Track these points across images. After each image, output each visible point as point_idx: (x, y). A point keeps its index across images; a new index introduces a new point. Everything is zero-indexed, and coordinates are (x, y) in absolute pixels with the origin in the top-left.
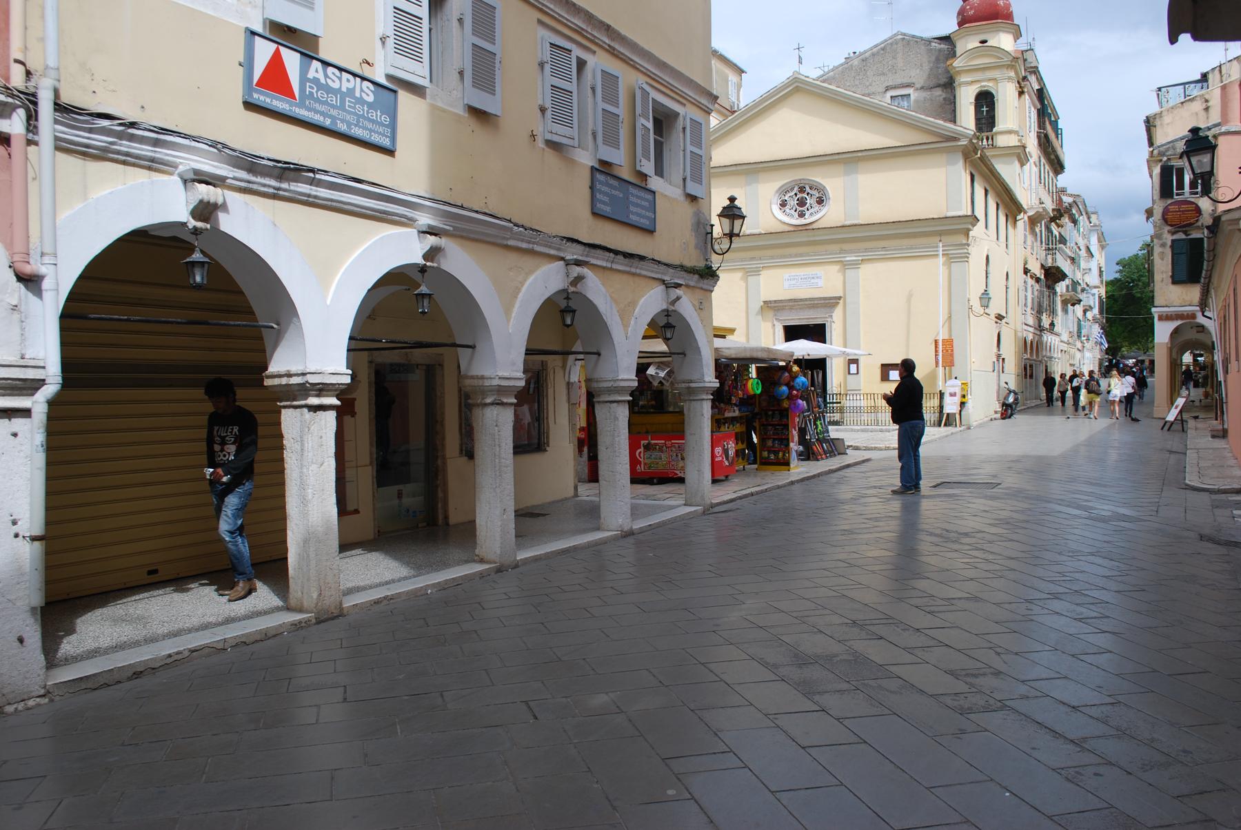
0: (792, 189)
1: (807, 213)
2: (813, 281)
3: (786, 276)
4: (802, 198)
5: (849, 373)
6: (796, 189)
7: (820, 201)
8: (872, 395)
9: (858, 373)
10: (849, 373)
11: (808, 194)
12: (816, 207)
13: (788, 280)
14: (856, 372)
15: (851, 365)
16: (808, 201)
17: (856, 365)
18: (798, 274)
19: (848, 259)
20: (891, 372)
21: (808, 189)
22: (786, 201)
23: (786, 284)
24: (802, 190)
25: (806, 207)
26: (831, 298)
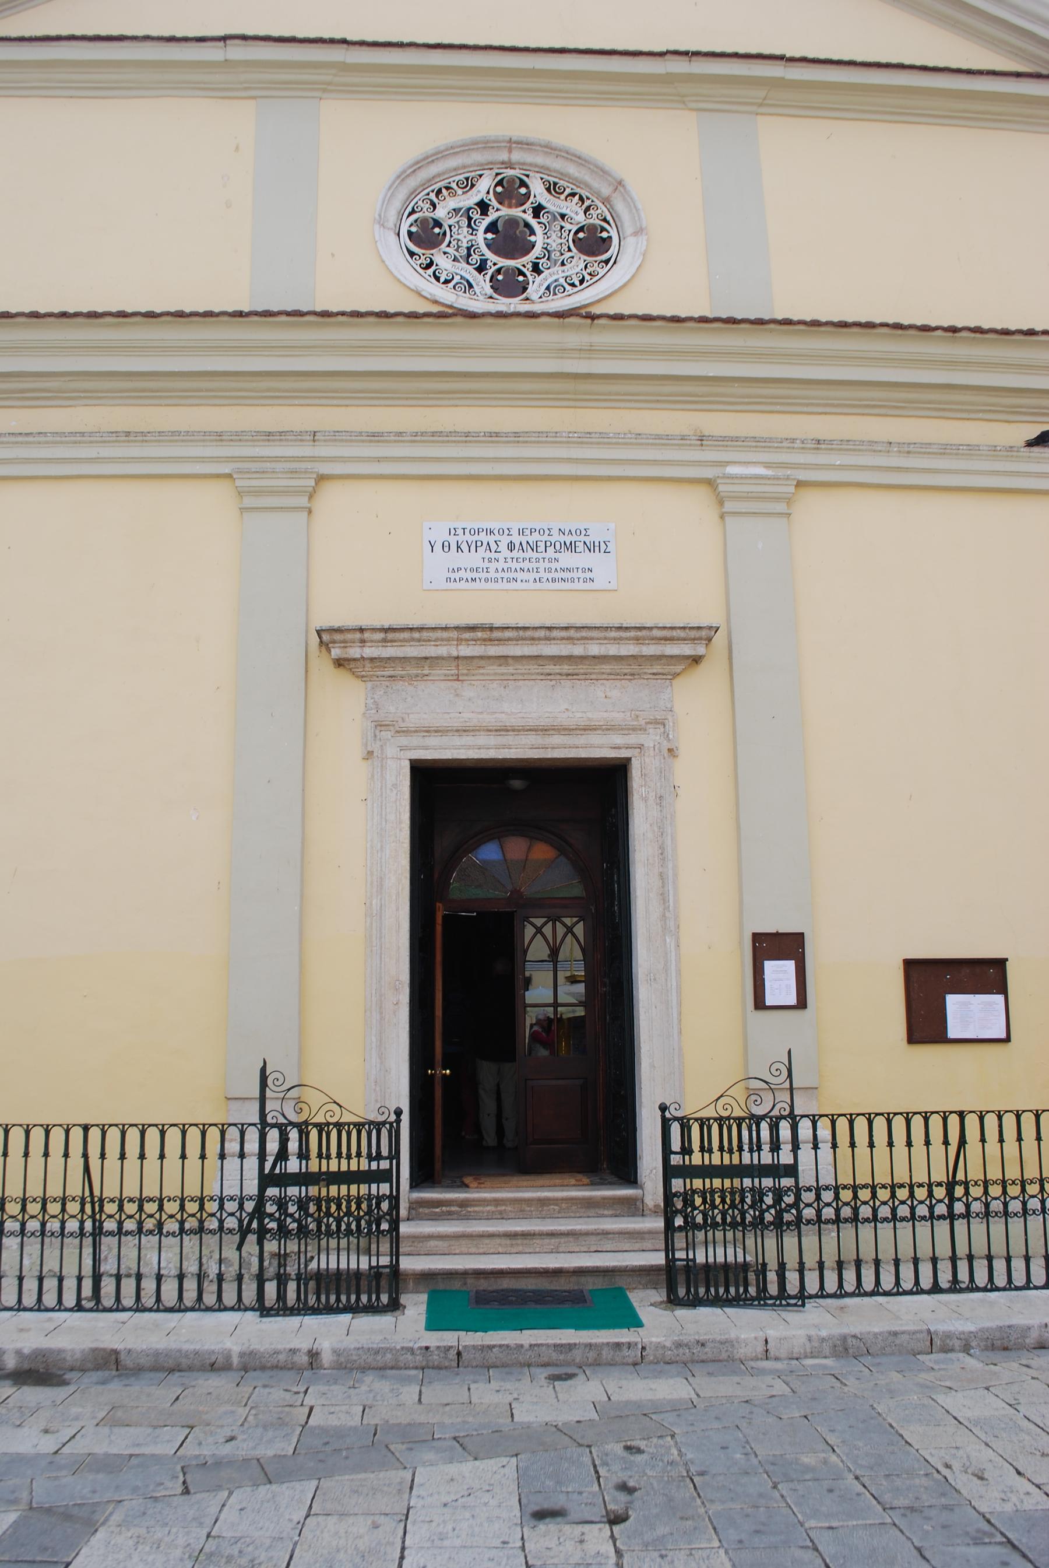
0: (469, 184)
1: (536, 286)
2: (567, 559)
4: (512, 222)
5: (760, 1003)
6: (485, 186)
8: (954, 1121)
9: (802, 1003)
11: (538, 211)
12: (578, 263)
13: (446, 547)
14: (792, 1000)
15: (770, 966)
16: (539, 239)
17: (790, 965)
18: (495, 525)
19: (731, 470)
20: (953, 1001)
21: (537, 188)
22: (438, 224)
25: (531, 256)
26: (669, 634)
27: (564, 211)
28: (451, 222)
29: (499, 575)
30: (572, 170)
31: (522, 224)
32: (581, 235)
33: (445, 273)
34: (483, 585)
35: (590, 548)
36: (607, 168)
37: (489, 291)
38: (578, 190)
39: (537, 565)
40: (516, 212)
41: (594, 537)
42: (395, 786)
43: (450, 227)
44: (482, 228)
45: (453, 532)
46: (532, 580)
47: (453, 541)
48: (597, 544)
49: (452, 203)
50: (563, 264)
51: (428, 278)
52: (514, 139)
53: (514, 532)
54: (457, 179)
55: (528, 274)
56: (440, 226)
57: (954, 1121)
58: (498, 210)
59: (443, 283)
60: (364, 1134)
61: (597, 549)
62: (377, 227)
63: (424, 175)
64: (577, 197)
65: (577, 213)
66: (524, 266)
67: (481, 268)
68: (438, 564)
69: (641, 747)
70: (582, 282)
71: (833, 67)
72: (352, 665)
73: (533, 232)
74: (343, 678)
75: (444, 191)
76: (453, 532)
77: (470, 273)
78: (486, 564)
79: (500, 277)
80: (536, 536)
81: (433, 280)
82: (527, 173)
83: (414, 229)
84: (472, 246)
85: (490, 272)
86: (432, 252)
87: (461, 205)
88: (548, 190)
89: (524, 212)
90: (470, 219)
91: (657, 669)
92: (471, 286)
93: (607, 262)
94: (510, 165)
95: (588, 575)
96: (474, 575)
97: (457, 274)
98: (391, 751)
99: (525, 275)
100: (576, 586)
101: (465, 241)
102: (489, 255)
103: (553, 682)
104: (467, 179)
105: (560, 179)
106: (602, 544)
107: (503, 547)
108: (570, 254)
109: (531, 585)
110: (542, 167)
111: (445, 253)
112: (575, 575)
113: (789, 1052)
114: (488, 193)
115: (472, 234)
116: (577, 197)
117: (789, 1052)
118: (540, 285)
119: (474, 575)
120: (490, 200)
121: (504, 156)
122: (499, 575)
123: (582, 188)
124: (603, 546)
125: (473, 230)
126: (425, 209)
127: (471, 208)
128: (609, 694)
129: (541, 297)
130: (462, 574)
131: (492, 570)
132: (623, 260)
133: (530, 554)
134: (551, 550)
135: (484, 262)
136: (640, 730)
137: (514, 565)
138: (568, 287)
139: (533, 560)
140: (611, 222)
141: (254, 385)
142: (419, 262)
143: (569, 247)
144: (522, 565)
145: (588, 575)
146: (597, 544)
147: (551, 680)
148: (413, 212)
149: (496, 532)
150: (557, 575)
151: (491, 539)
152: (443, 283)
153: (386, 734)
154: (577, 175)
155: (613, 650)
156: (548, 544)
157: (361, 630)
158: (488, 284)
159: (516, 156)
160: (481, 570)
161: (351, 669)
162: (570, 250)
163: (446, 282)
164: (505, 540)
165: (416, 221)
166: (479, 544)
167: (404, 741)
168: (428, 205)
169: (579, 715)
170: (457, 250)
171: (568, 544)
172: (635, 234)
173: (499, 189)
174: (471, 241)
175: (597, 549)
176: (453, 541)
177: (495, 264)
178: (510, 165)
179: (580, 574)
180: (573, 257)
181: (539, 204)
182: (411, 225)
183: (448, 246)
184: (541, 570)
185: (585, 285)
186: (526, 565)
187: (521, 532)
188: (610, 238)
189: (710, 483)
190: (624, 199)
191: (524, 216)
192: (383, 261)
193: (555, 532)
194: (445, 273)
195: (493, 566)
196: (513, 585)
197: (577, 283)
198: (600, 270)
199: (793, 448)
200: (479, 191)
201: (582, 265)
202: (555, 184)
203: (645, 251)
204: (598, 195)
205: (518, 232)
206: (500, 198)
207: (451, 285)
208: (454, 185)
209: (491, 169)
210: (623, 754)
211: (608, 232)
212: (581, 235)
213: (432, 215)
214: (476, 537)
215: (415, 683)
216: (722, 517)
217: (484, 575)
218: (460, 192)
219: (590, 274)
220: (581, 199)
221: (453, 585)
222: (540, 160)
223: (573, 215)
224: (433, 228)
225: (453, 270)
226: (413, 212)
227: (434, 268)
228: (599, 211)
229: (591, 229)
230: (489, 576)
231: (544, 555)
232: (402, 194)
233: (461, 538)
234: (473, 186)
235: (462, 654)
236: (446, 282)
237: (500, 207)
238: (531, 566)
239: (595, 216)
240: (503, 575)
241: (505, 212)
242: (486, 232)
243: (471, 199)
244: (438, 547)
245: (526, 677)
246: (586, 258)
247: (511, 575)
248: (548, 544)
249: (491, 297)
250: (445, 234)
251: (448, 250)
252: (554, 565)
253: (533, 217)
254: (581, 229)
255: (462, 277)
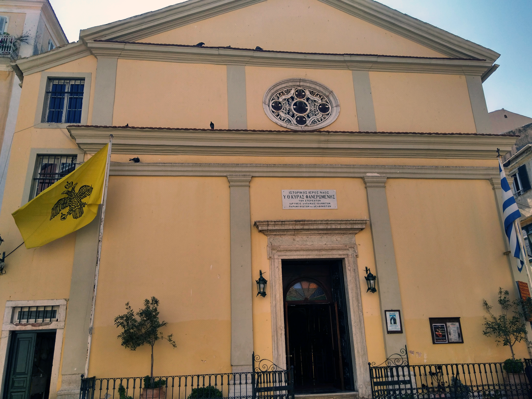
0: (288, 92)
1: (309, 122)
2: (323, 200)
3: (286, 192)
4: (301, 103)
6: (293, 91)
7: (324, 109)
8: (454, 366)
10: (401, 332)
11: (308, 99)
12: (320, 115)
16: (308, 108)
19: (368, 174)
21: (307, 93)
22: (280, 103)
23: (286, 202)
24: (300, 94)
26: (354, 222)
27: (315, 100)
28: (284, 102)
29: (304, 205)
30: (318, 88)
31: (304, 103)
32: (320, 107)
33: (283, 117)
34: (299, 208)
35: (329, 197)
36: (328, 88)
37: (296, 123)
38: (319, 94)
39: (315, 202)
40: (302, 100)
41: (330, 194)
42: (277, 267)
43: (283, 104)
44: (292, 105)
45: (290, 193)
46: (313, 206)
47: (290, 195)
48: (331, 196)
49: (284, 97)
50: (316, 115)
51: (278, 119)
52: (301, 79)
53: (308, 192)
54: (285, 90)
55: (306, 118)
56: (281, 104)
57: (454, 366)
58: (297, 99)
59: (282, 120)
60: (265, 375)
61: (331, 197)
62: (264, 104)
63: (275, 89)
64: (319, 96)
65: (319, 100)
66: (305, 115)
67: (293, 116)
68: (286, 202)
69: (347, 255)
70: (321, 120)
71: (391, 58)
72: (264, 231)
73: (307, 106)
74: (262, 236)
75: (281, 93)
76: (290, 193)
77: (289, 117)
78: (300, 202)
79: (298, 119)
80: (314, 194)
81: (279, 120)
82: (305, 88)
83: (273, 105)
84: (290, 109)
85: (296, 117)
86: (279, 111)
87: (286, 98)
88: (310, 93)
89: (304, 100)
90: (289, 102)
91: (351, 232)
92: (290, 121)
93: (328, 114)
94: (300, 86)
95: (329, 205)
96: (297, 205)
97: (286, 118)
98: (276, 257)
99: (305, 118)
100: (326, 208)
101: (288, 108)
102: (295, 112)
103: (321, 236)
104: (287, 90)
105: (314, 90)
106: (332, 196)
107: (305, 197)
108: (318, 112)
109: (313, 208)
110: (309, 87)
111: (282, 112)
112: (325, 205)
113: (406, 346)
114: (294, 94)
115: (289, 106)
116: (319, 96)
117: (406, 346)
118: (310, 121)
119: (297, 205)
120: (294, 96)
121: (298, 84)
122: (304, 205)
123: (320, 93)
124: (333, 197)
125: (290, 105)
126: (276, 99)
127: (289, 99)
128: (337, 239)
129: (310, 125)
130: (293, 205)
131: (302, 204)
132: (334, 114)
133: (312, 199)
134: (318, 198)
135: (293, 114)
136: (347, 250)
137: (308, 202)
138: (318, 122)
139: (313, 201)
140: (329, 103)
141: (232, 150)
142: (275, 114)
143: (317, 110)
144: (310, 202)
145: (329, 205)
146: (331, 196)
147: (320, 235)
148: (273, 100)
149: (302, 193)
150: (320, 205)
151: (301, 195)
152: (282, 120)
153: (275, 252)
154: (319, 89)
155: (339, 227)
156: (317, 196)
157: (268, 222)
158: (295, 121)
159: (302, 84)
160: (299, 204)
161: (263, 233)
162: (317, 111)
163: (283, 120)
164: (305, 195)
165: (274, 102)
166: (298, 196)
167: (279, 253)
168: (277, 98)
169: (329, 245)
170: (286, 111)
171: (323, 196)
172: (336, 106)
173: (297, 93)
174: (290, 108)
175: (331, 197)
176: (290, 195)
177: (297, 115)
178: (300, 86)
179: (327, 205)
180: (318, 113)
181: (308, 97)
182: (272, 104)
183: (283, 110)
184: (316, 203)
185: (322, 121)
186: (311, 202)
187: (310, 193)
188: (329, 107)
189: (362, 178)
190: (333, 96)
191: (304, 101)
192: (266, 114)
193: (319, 192)
194: (283, 117)
195: (302, 202)
196: (308, 208)
197: (320, 121)
198: (326, 117)
199: (385, 168)
200: (291, 94)
201: (321, 115)
202: (312, 91)
203: (340, 111)
204: (325, 95)
205: (302, 106)
206: (297, 96)
207: (285, 121)
208: (284, 92)
209: (294, 87)
210: (342, 257)
211: (328, 106)
212: (320, 107)
213: (278, 100)
214: (297, 194)
215: (282, 237)
216: (366, 188)
217: (300, 205)
218: (286, 94)
219: (324, 118)
220: (320, 96)
221: (291, 208)
222: (308, 85)
223: (318, 101)
224: (279, 104)
225: (285, 117)
226: (273, 100)
227: (279, 116)
228: (325, 100)
229: (323, 105)
230: (301, 205)
231: (316, 199)
232: (270, 95)
233: (293, 194)
234: (289, 92)
235: (296, 228)
236: (283, 120)
237: (297, 98)
238: (313, 202)
239: (324, 101)
240: (305, 205)
241: (298, 100)
242: (293, 106)
243: (289, 96)
244: (286, 197)
245: (313, 235)
246: (322, 113)
247: (308, 205)
248: (317, 196)
249: (296, 125)
250: (282, 106)
251: (283, 111)
252: (319, 202)
253: (307, 101)
254: (320, 105)
255: (288, 119)
